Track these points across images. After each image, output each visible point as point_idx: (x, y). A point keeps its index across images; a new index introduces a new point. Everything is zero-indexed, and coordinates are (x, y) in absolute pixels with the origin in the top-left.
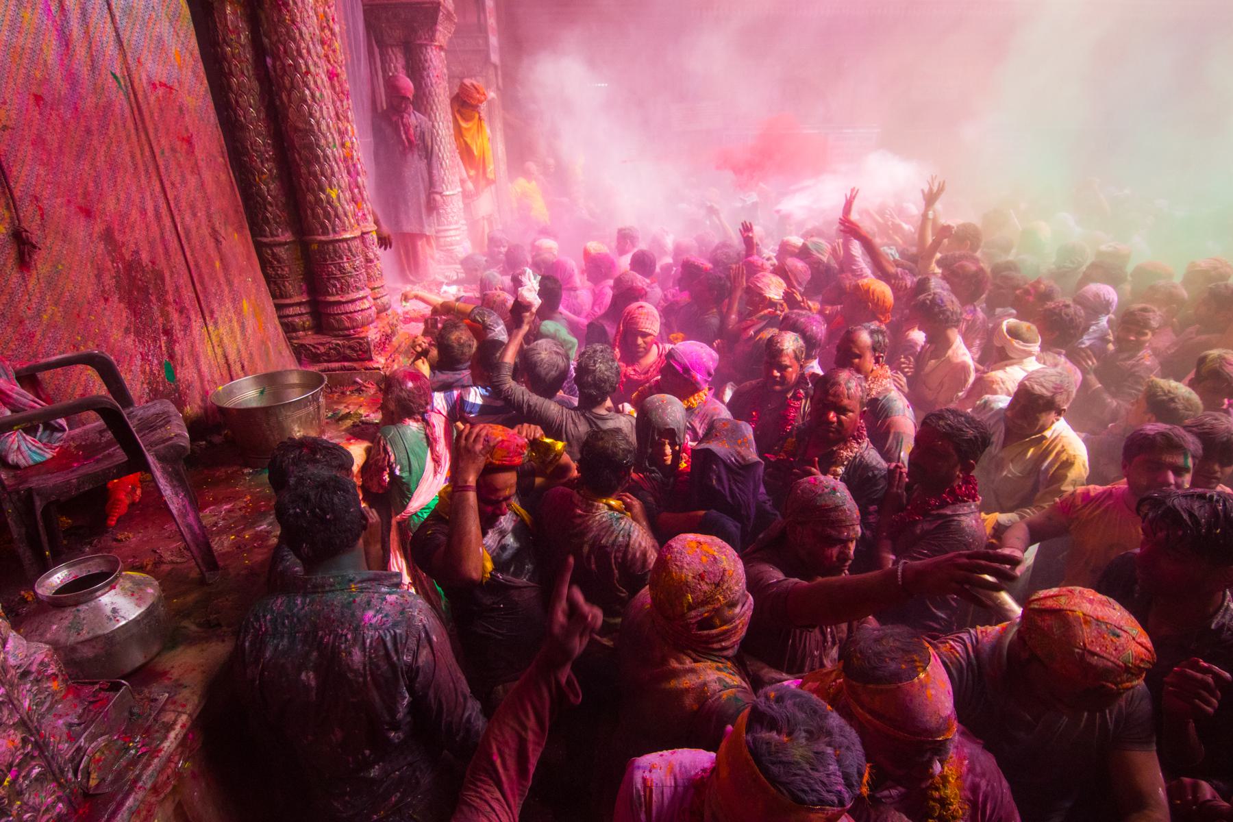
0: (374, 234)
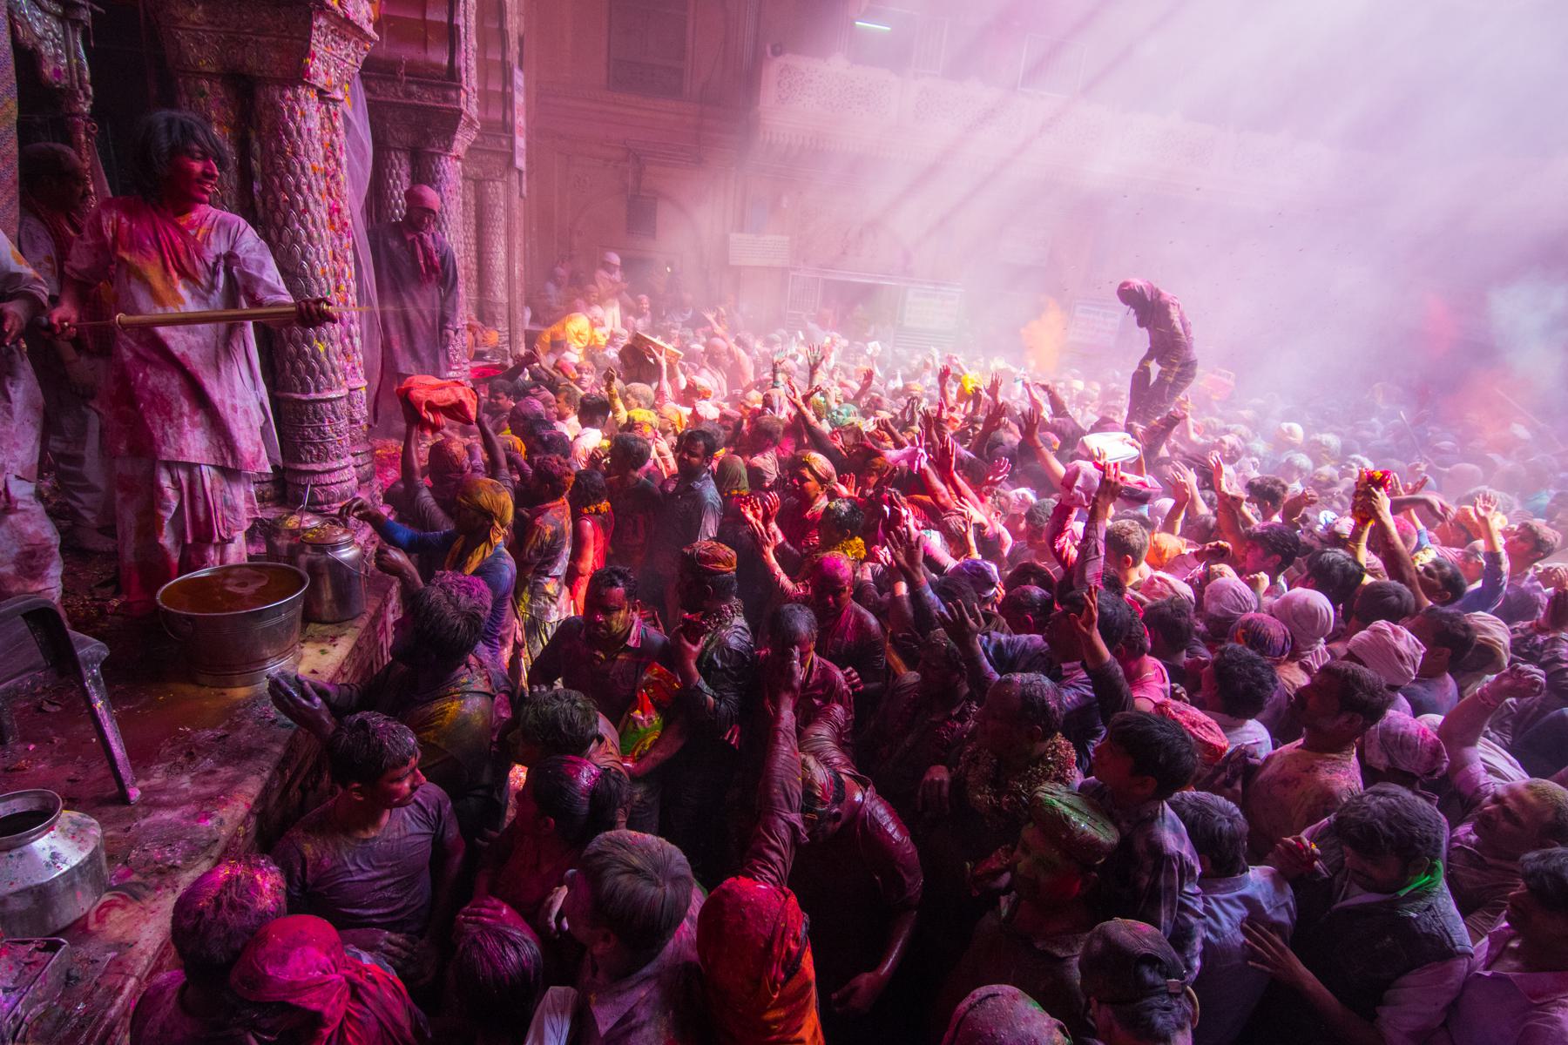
0: (364, 391)
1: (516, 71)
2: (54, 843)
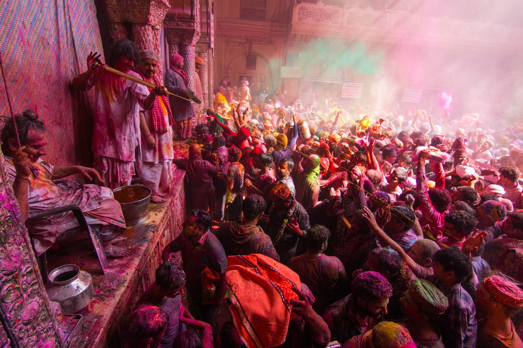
1: (211, 15)
2: (78, 283)
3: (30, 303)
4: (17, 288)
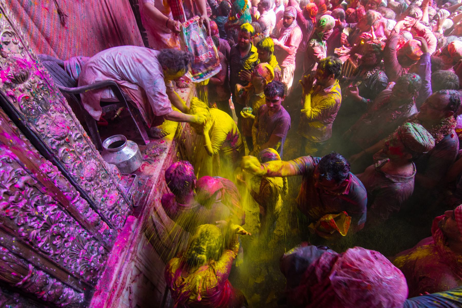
3: (89, 164)
4: (72, 151)
